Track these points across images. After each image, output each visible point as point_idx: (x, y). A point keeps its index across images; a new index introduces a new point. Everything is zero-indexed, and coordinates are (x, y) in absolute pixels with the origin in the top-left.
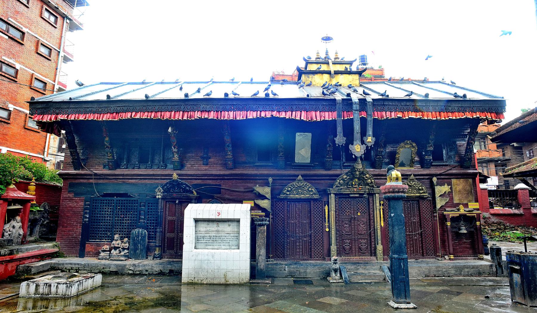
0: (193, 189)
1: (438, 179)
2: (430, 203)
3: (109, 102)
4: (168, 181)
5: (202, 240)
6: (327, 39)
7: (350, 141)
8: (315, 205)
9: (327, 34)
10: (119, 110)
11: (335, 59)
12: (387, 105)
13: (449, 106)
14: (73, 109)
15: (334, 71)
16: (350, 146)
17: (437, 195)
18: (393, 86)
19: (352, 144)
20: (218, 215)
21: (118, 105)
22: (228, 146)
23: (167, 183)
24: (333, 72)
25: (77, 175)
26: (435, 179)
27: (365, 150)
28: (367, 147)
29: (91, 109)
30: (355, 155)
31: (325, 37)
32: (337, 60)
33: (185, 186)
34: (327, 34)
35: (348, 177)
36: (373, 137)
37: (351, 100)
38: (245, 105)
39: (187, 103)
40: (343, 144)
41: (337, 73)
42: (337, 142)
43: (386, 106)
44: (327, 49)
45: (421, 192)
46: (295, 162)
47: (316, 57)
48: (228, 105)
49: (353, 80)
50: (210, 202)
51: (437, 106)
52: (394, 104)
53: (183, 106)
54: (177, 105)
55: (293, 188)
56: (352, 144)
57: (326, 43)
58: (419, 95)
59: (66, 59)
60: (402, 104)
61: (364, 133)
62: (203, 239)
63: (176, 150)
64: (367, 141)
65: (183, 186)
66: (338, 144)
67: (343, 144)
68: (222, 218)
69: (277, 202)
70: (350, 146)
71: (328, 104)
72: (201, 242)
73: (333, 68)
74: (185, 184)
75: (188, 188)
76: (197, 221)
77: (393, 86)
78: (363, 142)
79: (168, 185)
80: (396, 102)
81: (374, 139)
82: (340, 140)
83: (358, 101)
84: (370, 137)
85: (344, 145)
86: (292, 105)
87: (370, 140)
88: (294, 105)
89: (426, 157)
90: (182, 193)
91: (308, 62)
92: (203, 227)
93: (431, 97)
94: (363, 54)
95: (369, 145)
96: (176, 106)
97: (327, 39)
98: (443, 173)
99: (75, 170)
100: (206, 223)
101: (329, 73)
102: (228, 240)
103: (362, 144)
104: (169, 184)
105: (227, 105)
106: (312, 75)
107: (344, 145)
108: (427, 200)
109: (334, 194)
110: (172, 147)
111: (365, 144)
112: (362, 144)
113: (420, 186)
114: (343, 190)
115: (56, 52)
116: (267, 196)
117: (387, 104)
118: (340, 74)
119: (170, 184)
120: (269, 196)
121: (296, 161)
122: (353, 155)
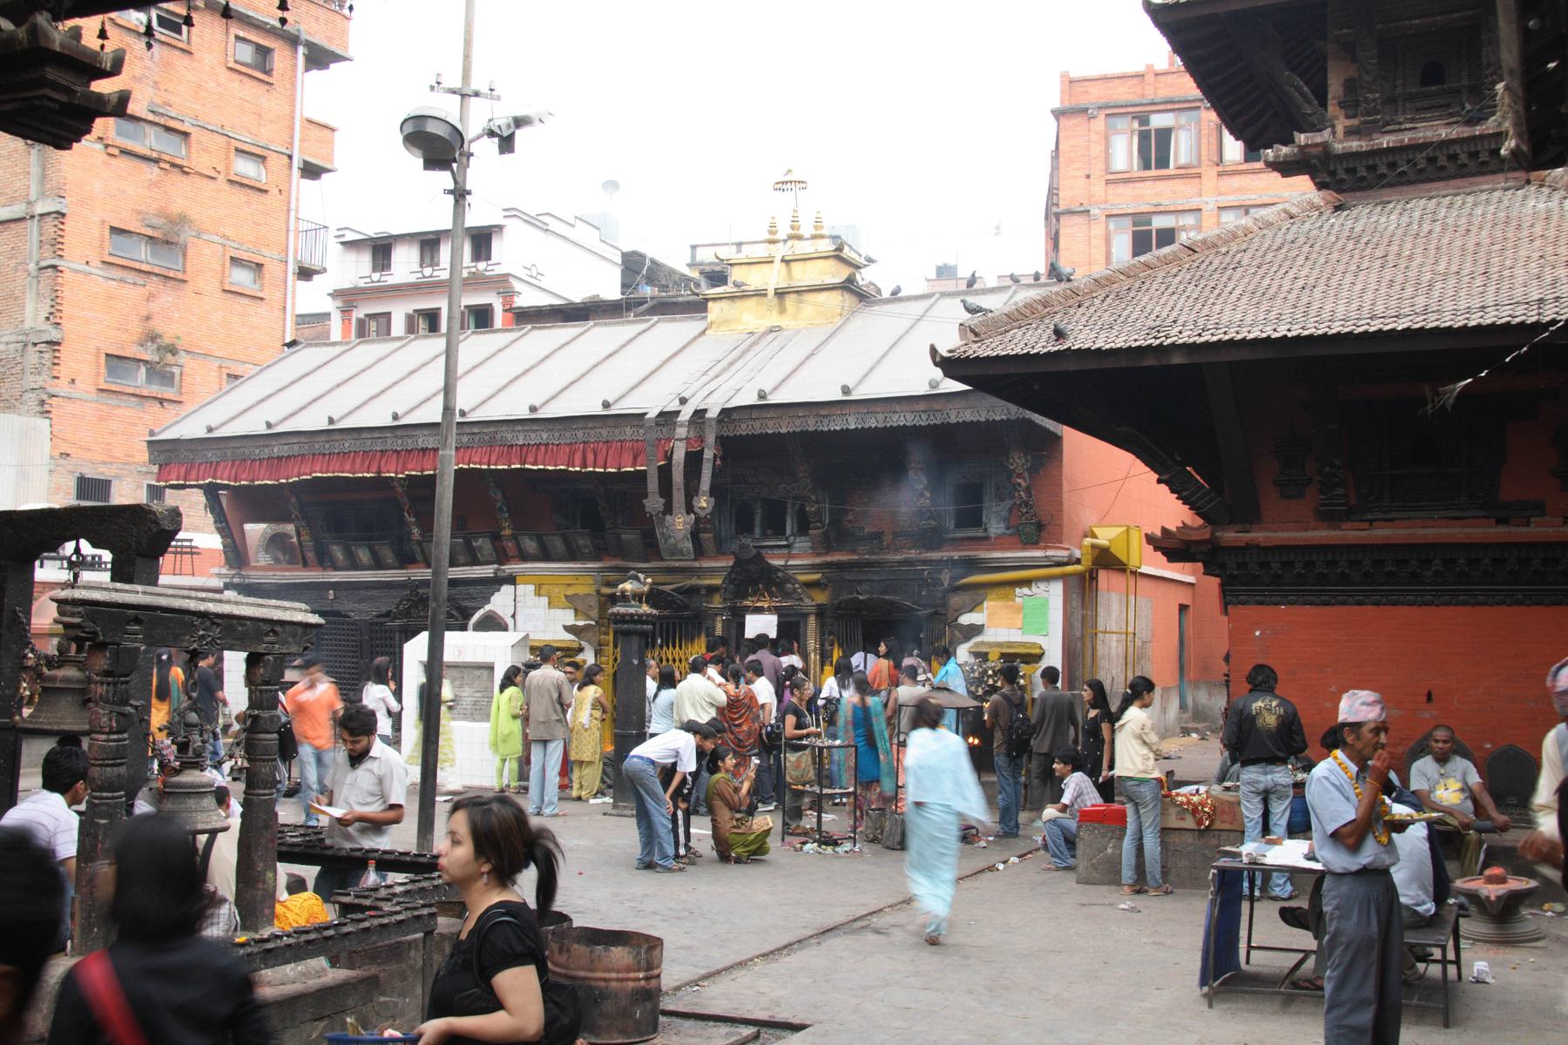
14: (214, 452)
16: (668, 517)
19: (671, 515)
21: (284, 442)
22: (501, 509)
28: (698, 520)
29: (242, 450)
59: (312, 171)
61: (691, 492)
63: (413, 520)
68: (466, 660)
78: (689, 509)
82: (653, 503)
87: (703, 502)
103: (688, 513)
111: (695, 514)
112: (688, 513)
115: (286, 159)
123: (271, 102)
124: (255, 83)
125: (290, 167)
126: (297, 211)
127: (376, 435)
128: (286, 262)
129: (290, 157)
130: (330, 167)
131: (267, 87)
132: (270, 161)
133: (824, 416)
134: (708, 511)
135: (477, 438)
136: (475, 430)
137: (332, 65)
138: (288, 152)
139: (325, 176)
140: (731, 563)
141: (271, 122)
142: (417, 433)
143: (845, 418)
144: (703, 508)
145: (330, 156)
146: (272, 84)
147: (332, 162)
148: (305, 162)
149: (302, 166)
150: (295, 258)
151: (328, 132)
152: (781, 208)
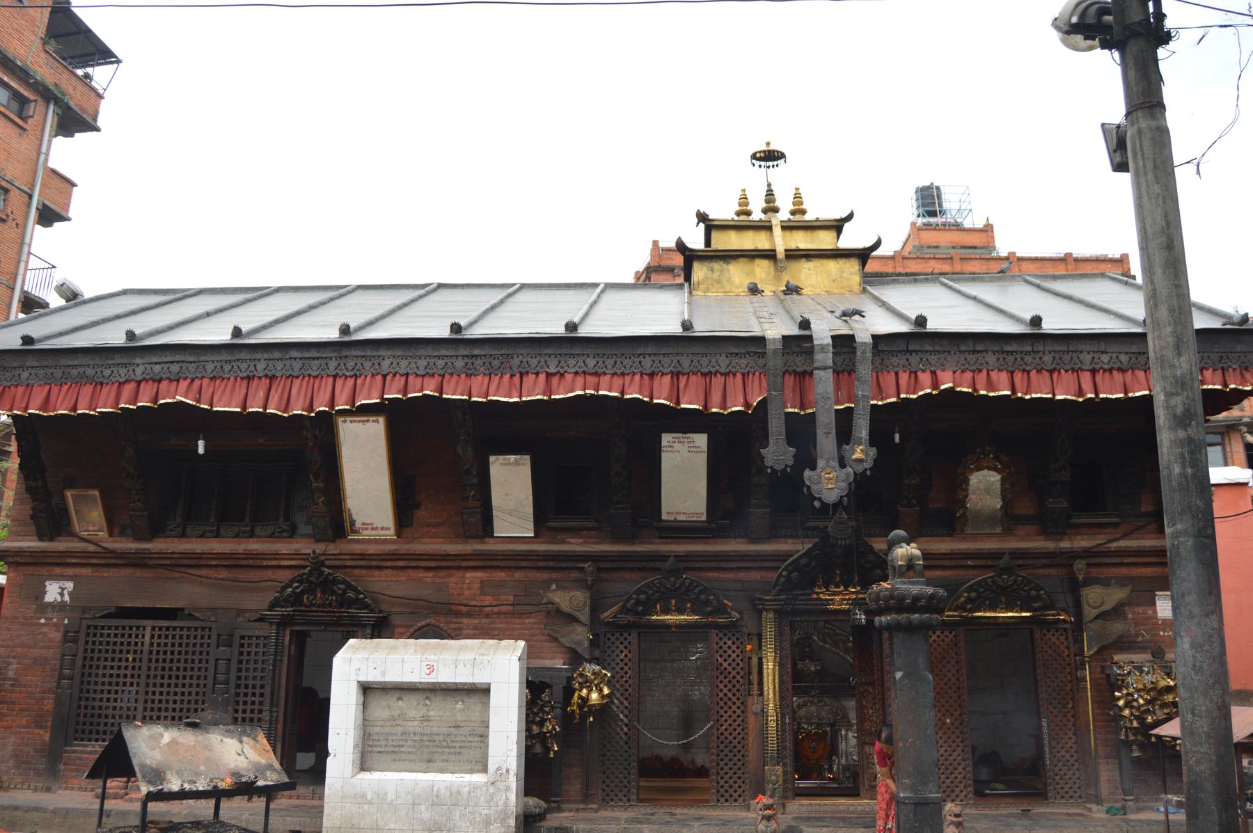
0: (366, 597)
1: (1088, 565)
2: (1066, 639)
3: (133, 350)
4: (296, 573)
5: (381, 746)
6: (770, 156)
7: (806, 459)
8: (721, 643)
9: (768, 144)
10: (157, 371)
11: (793, 213)
12: (916, 352)
13: (1102, 353)
14: (33, 371)
15: (786, 250)
16: (807, 473)
17: (1089, 613)
18: (959, 292)
19: (813, 468)
20: (428, 671)
21: (155, 360)
23: (292, 581)
24: (781, 254)
25: (44, 553)
26: (1080, 566)
27: (850, 484)
29: (81, 370)
30: (820, 499)
31: (760, 152)
32: (798, 217)
33: (342, 587)
34: (768, 144)
35: (813, 563)
36: (871, 445)
37: (810, 338)
38: (508, 355)
39: (345, 353)
40: (787, 466)
41: (794, 255)
42: (768, 462)
43: (914, 354)
44: (769, 185)
45: (1036, 605)
46: (660, 520)
47: (738, 208)
48: (460, 358)
49: (841, 277)
50: (417, 634)
51: (1068, 352)
52: (937, 348)
53: (334, 359)
54: (317, 358)
55: (653, 594)
56: (813, 468)
57: (769, 167)
58: (1018, 320)
59: (49, 217)
60: (963, 348)
62: (384, 743)
64: (854, 457)
65: (339, 589)
66: (771, 467)
67: (787, 466)
68: (440, 680)
69: (609, 635)
70: (807, 473)
71: (744, 351)
72: (379, 749)
73: (781, 242)
74: (344, 582)
75: (351, 594)
76: (366, 689)
77: (959, 292)
79: (296, 585)
80: (945, 342)
81: (873, 452)
83: (829, 341)
84: (861, 447)
85: (789, 470)
86: (640, 355)
87: (860, 452)
88: (647, 356)
89: (1051, 500)
90: (335, 607)
91: (710, 226)
92: (382, 709)
93: (1048, 326)
94: (928, 184)
95: (859, 469)
96: (316, 362)
97: (770, 156)
98: (1093, 547)
99: (41, 539)
100: (397, 694)
101: (770, 255)
102: (458, 745)
104: (298, 582)
105: (457, 357)
106: (721, 263)
107: (789, 470)
108: (1057, 631)
109: (775, 611)
110: (311, 476)
113: (1031, 589)
114: (802, 600)
116: (578, 614)
117: (917, 347)
118: (804, 260)
119: (301, 582)
120: (584, 616)
121: (664, 517)
122: (815, 498)
123: (21, 145)
124: (9, 124)
125: (29, 205)
126: (30, 246)
127: (314, 354)
128: (13, 289)
129: (30, 197)
130: (63, 213)
131: (21, 131)
132: (12, 194)
133: (1011, 352)
134: (868, 465)
135: (479, 362)
136: (476, 352)
137: (77, 135)
138: (29, 191)
139: (56, 225)
140: (808, 546)
141: (18, 161)
142: (382, 353)
143: (1038, 356)
144: (860, 461)
145: (67, 206)
146: (25, 130)
147: (67, 211)
148: (44, 205)
149: (40, 207)
150: (22, 288)
151: (69, 186)
152: (755, 181)
